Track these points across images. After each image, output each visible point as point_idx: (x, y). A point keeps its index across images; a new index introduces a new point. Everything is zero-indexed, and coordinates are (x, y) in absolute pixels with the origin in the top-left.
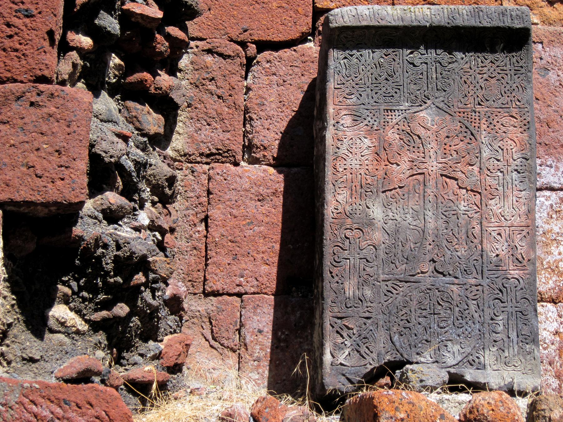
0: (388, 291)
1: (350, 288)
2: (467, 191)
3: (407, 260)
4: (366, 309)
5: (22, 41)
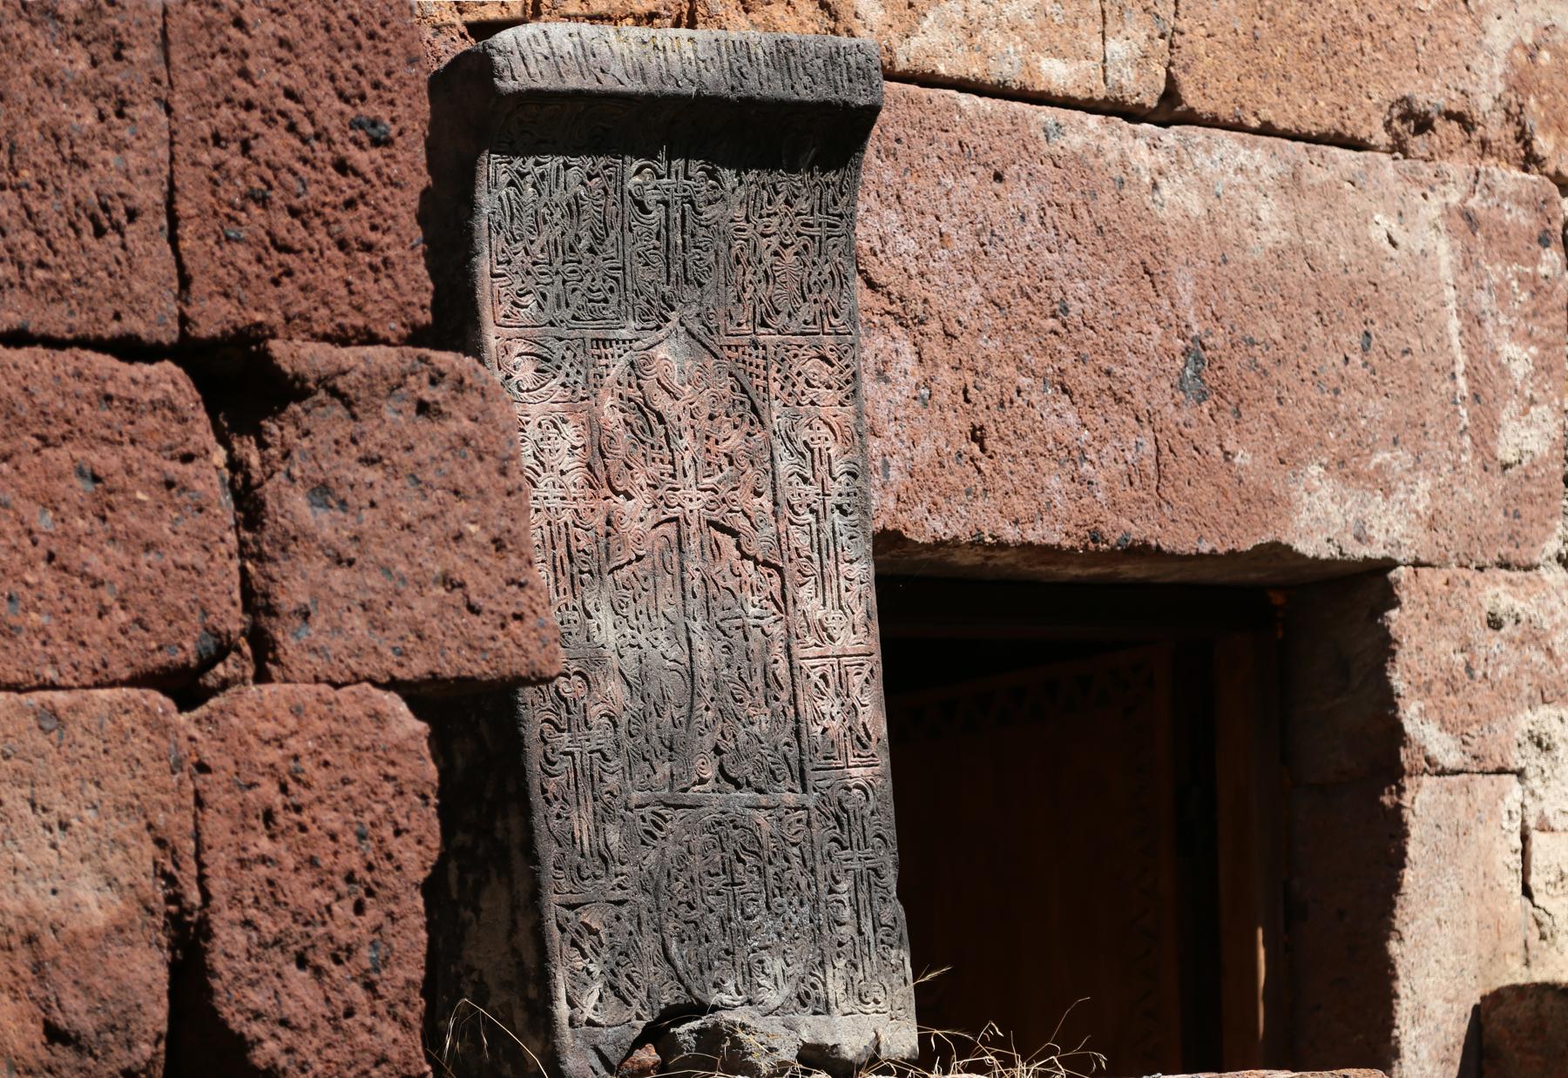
0: (647, 832)
2: (757, 563)
3: (671, 749)
4: (615, 881)
5: (378, 220)
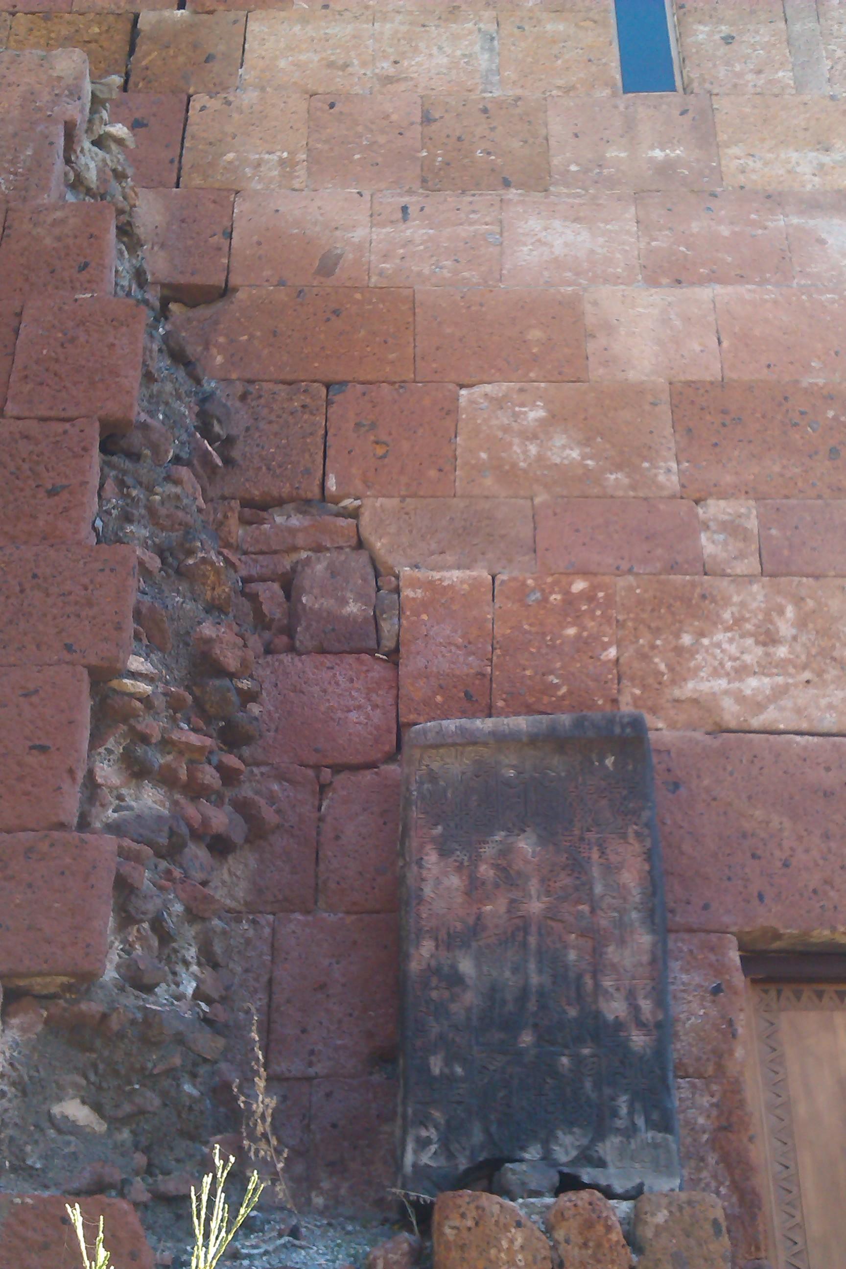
1: (436, 1065)
